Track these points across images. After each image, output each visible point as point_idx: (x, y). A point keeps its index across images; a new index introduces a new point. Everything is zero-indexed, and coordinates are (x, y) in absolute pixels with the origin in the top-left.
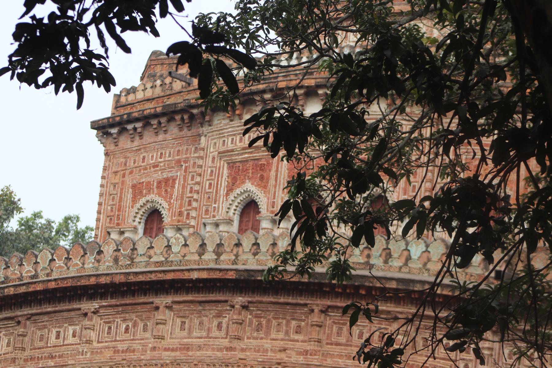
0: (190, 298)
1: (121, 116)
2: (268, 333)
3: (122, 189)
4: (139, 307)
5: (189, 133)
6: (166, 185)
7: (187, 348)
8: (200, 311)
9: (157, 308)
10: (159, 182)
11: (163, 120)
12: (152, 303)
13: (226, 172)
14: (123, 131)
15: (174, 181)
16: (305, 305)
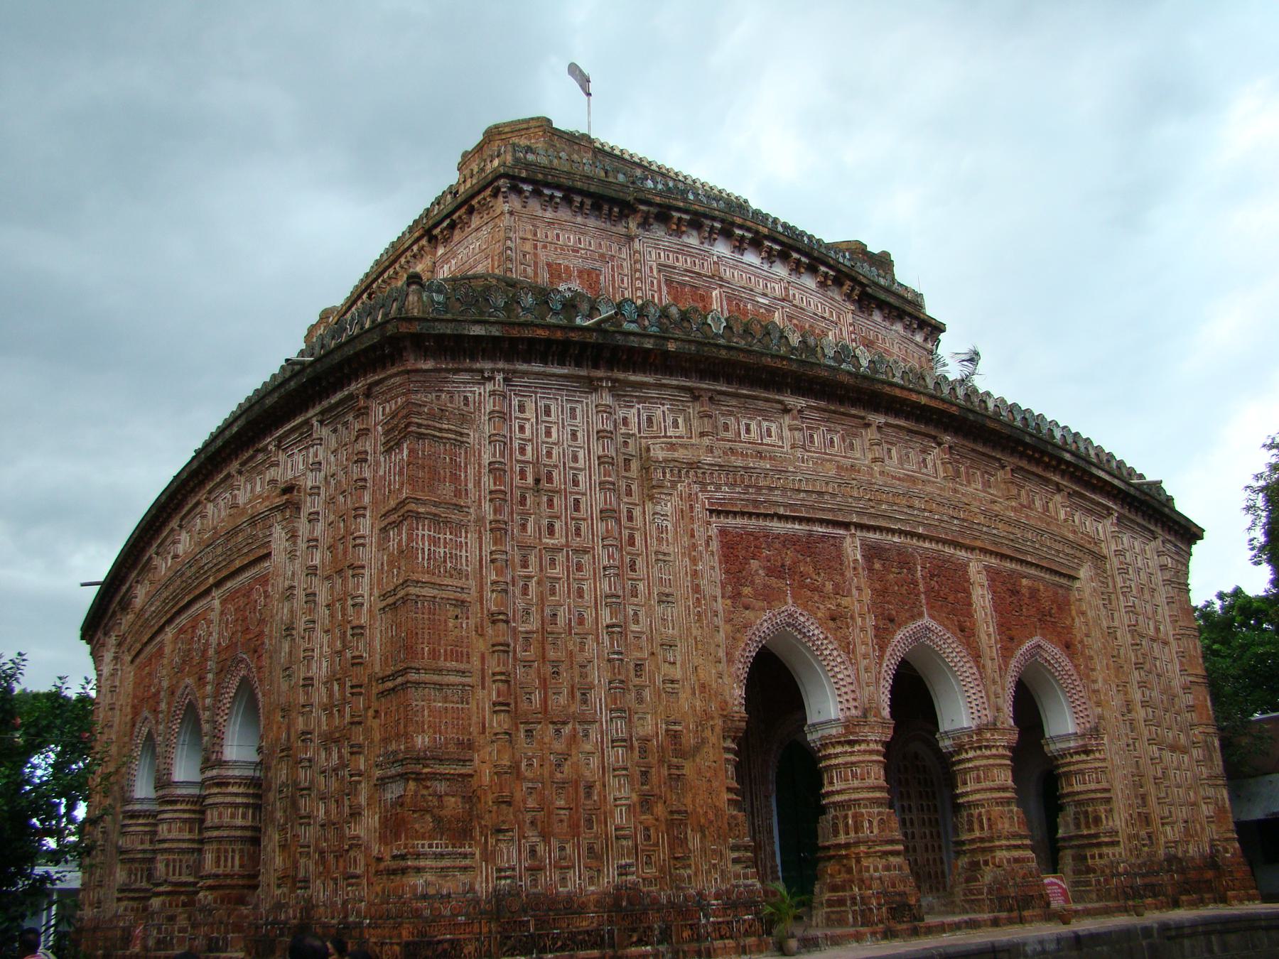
0: (902, 423)
1: (545, 175)
2: (969, 482)
3: (536, 263)
4: (847, 421)
5: (614, 229)
6: (590, 276)
7: (913, 480)
8: (907, 441)
9: (868, 425)
10: (580, 272)
11: (588, 202)
12: (863, 418)
13: (664, 288)
14: (537, 193)
15: (598, 276)
16: (999, 460)
